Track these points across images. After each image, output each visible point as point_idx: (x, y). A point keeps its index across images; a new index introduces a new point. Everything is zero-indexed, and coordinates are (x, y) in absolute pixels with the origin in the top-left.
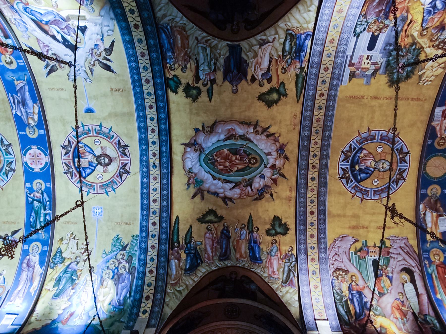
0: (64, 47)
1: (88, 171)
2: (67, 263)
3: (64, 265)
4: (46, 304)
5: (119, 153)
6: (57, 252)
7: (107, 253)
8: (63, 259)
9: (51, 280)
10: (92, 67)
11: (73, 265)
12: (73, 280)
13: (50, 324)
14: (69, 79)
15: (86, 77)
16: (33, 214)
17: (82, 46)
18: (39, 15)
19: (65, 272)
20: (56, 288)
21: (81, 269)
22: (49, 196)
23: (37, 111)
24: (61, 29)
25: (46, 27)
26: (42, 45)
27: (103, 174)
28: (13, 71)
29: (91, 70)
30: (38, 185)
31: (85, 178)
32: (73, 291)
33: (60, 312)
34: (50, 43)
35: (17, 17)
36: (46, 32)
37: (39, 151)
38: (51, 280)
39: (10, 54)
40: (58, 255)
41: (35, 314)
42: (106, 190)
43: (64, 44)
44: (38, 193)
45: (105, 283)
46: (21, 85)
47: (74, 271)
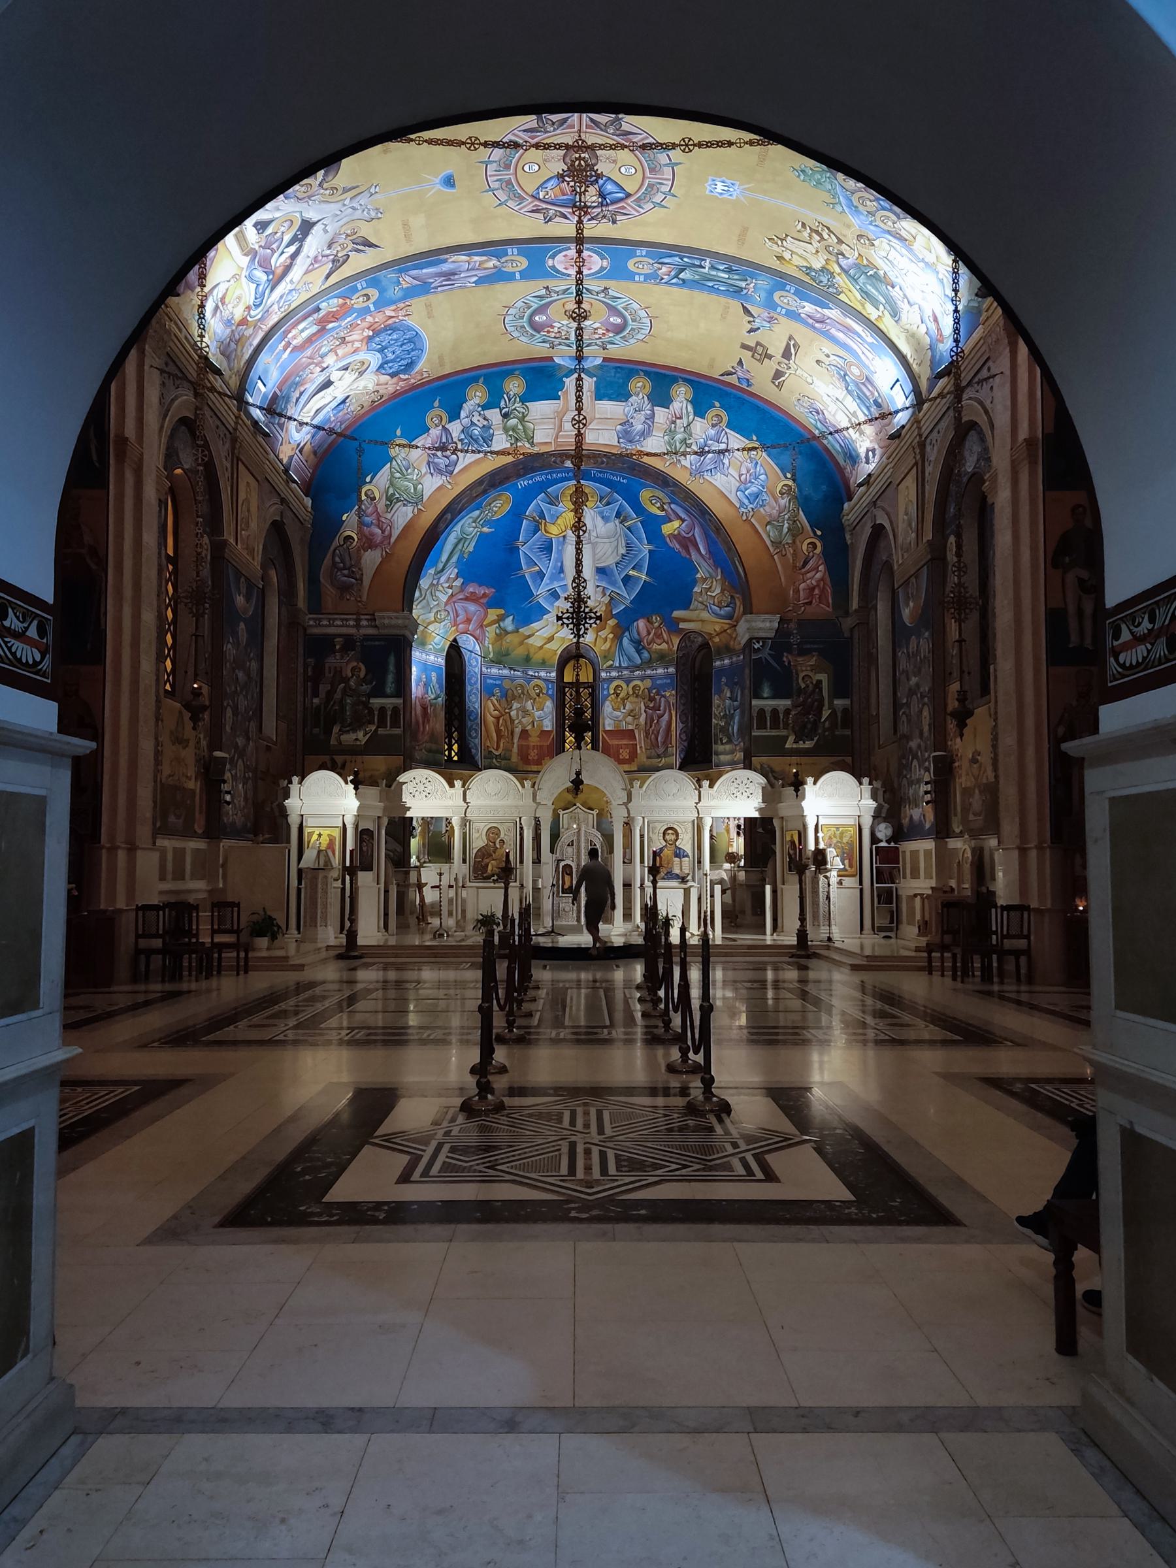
0: (309, 238)
1: (610, 187)
2: (838, 270)
3: (839, 274)
4: (903, 336)
5: (558, 132)
6: (807, 274)
7: (833, 201)
8: (824, 269)
9: (863, 306)
10: (340, 192)
11: (843, 262)
12: (876, 277)
13: (933, 356)
14: (379, 218)
15: (367, 194)
16: (710, 284)
17: (298, 215)
18: (261, 288)
19: (855, 280)
20: (881, 308)
21: (857, 255)
22: (671, 256)
23: (464, 258)
24: (273, 251)
25: (279, 271)
26: (316, 266)
27: (619, 165)
28: (382, 291)
29: (346, 190)
30: (641, 266)
31: (629, 195)
32: (897, 288)
33: (923, 329)
34: (308, 257)
35: (275, 307)
36: (288, 269)
37: (560, 257)
38: (863, 306)
39: (348, 301)
40: (814, 274)
41: (911, 361)
42: (665, 165)
43: (302, 240)
44: (660, 269)
45: (903, 233)
46: (408, 279)
47: (857, 266)
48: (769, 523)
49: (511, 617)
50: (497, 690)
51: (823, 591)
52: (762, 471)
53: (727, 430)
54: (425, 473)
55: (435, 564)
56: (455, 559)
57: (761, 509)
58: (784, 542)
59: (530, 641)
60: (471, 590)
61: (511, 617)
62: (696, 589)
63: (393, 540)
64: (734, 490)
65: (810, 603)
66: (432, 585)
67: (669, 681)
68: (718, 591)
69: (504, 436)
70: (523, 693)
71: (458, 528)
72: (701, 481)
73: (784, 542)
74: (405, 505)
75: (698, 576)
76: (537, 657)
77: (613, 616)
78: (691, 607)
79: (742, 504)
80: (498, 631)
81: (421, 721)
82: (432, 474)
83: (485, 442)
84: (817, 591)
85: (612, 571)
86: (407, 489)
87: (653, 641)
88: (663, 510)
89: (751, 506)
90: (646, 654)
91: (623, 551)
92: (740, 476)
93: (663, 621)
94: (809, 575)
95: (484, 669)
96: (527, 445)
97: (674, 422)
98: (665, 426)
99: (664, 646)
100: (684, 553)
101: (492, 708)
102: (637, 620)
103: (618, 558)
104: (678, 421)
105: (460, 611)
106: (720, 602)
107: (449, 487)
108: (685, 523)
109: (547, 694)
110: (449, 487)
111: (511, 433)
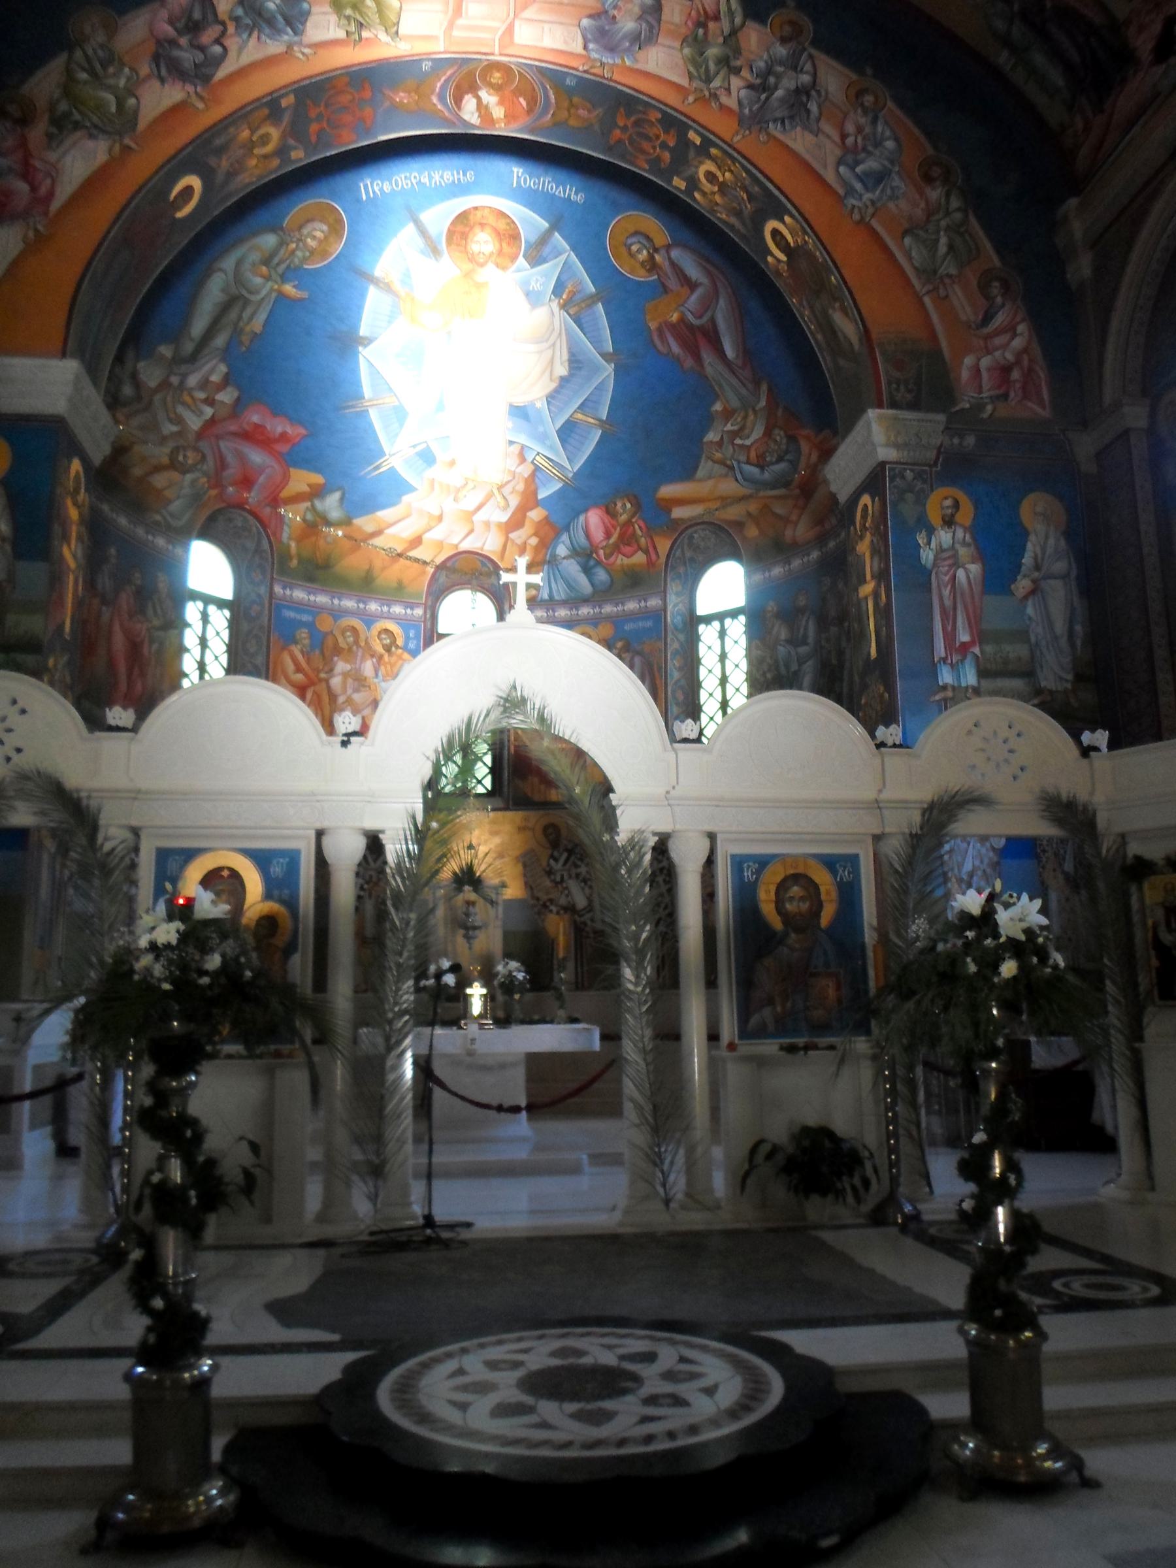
48: (906, 232)
49: (337, 496)
50: (303, 634)
51: (1029, 374)
52: (888, 133)
53: (813, 51)
54: (148, 77)
55: (176, 335)
56: (220, 341)
57: (891, 205)
58: (942, 271)
59: (378, 541)
60: (255, 418)
61: (337, 496)
62: (712, 436)
63: (56, 205)
64: (831, 161)
65: (1005, 396)
66: (165, 385)
67: (649, 624)
68: (758, 432)
69: (333, 18)
70: (356, 642)
71: (229, 263)
72: (763, 137)
73: (942, 271)
74: (91, 136)
75: (718, 407)
76: (390, 575)
77: (537, 503)
78: (700, 473)
79: (850, 191)
80: (309, 517)
81: (122, 668)
82: (162, 81)
83: (289, 22)
84: (1016, 375)
85: (538, 411)
86: (100, 107)
87: (616, 549)
88: (651, 266)
89: (867, 196)
90: (602, 575)
91: (562, 370)
92: (844, 137)
93: (638, 506)
94: (998, 341)
95: (278, 589)
96: (383, 37)
97: (704, 26)
98: (683, 30)
99: (639, 558)
100: (689, 363)
101: (290, 667)
102: (586, 510)
103: (553, 385)
104: (711, 25)
105: (230, 458)
106: (761, 457)
107: (201, 105)
108: (699, 292)
109: (405, 648)
110: (201, 105)
111: (349, 12)
